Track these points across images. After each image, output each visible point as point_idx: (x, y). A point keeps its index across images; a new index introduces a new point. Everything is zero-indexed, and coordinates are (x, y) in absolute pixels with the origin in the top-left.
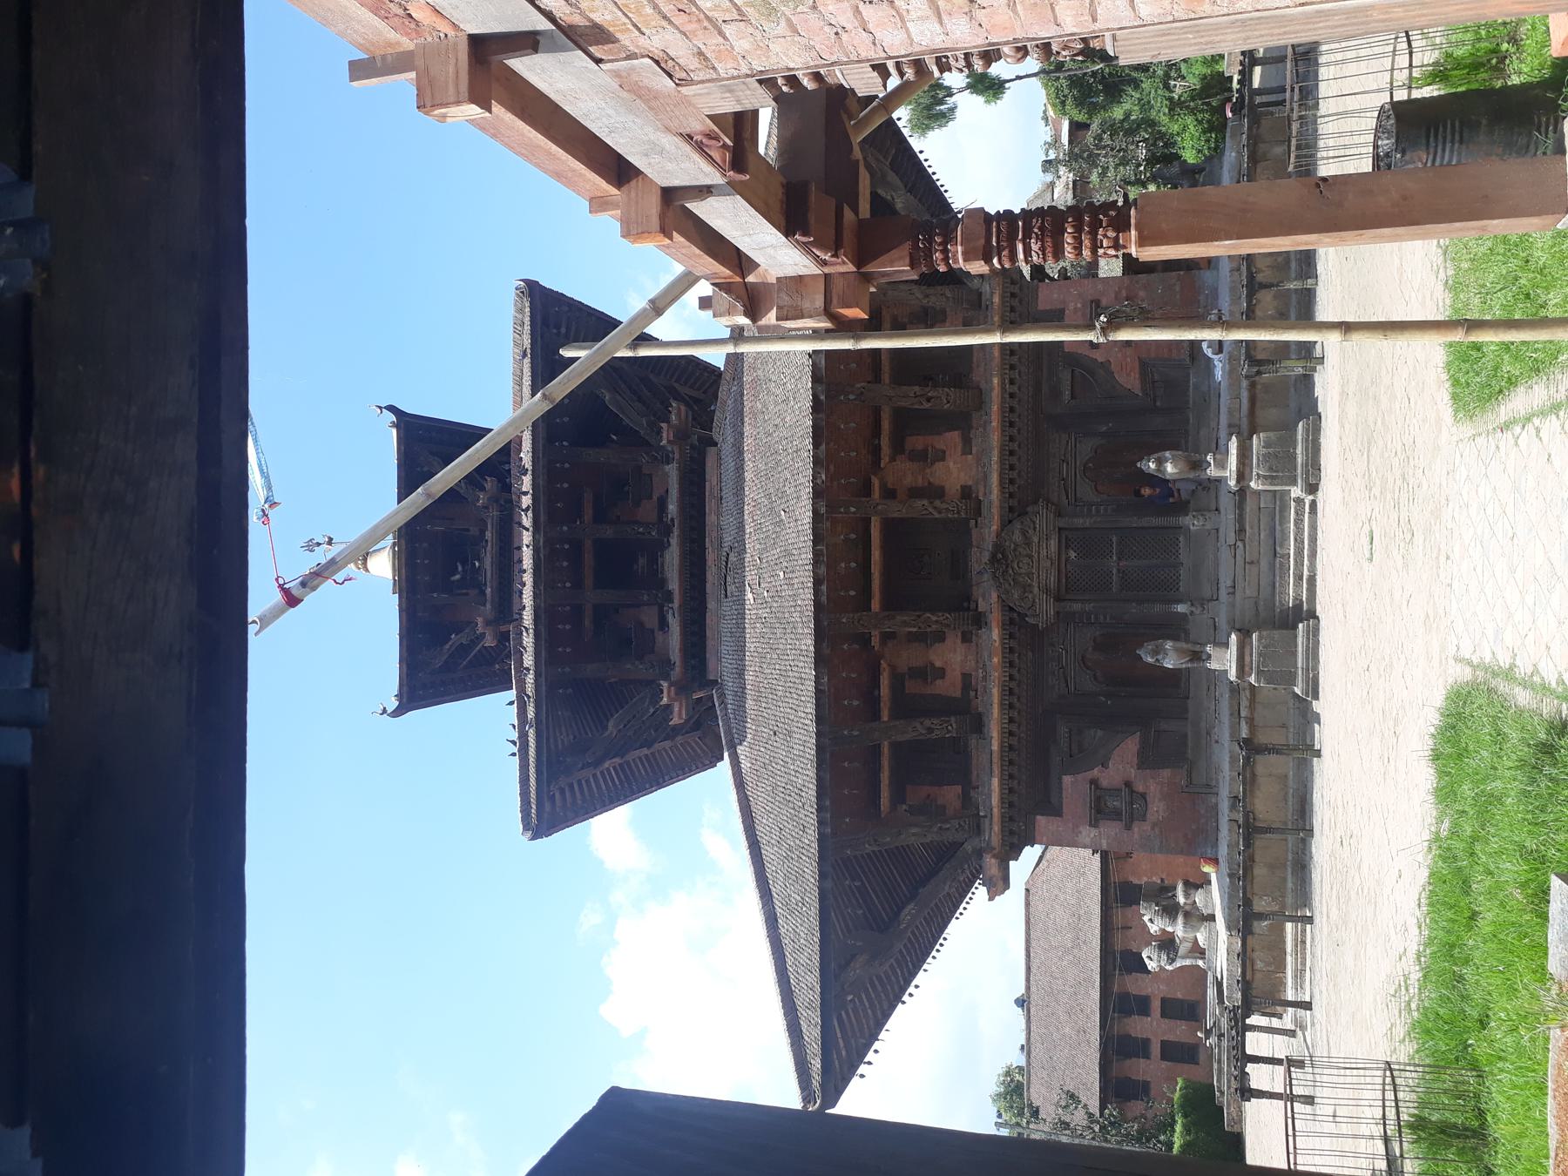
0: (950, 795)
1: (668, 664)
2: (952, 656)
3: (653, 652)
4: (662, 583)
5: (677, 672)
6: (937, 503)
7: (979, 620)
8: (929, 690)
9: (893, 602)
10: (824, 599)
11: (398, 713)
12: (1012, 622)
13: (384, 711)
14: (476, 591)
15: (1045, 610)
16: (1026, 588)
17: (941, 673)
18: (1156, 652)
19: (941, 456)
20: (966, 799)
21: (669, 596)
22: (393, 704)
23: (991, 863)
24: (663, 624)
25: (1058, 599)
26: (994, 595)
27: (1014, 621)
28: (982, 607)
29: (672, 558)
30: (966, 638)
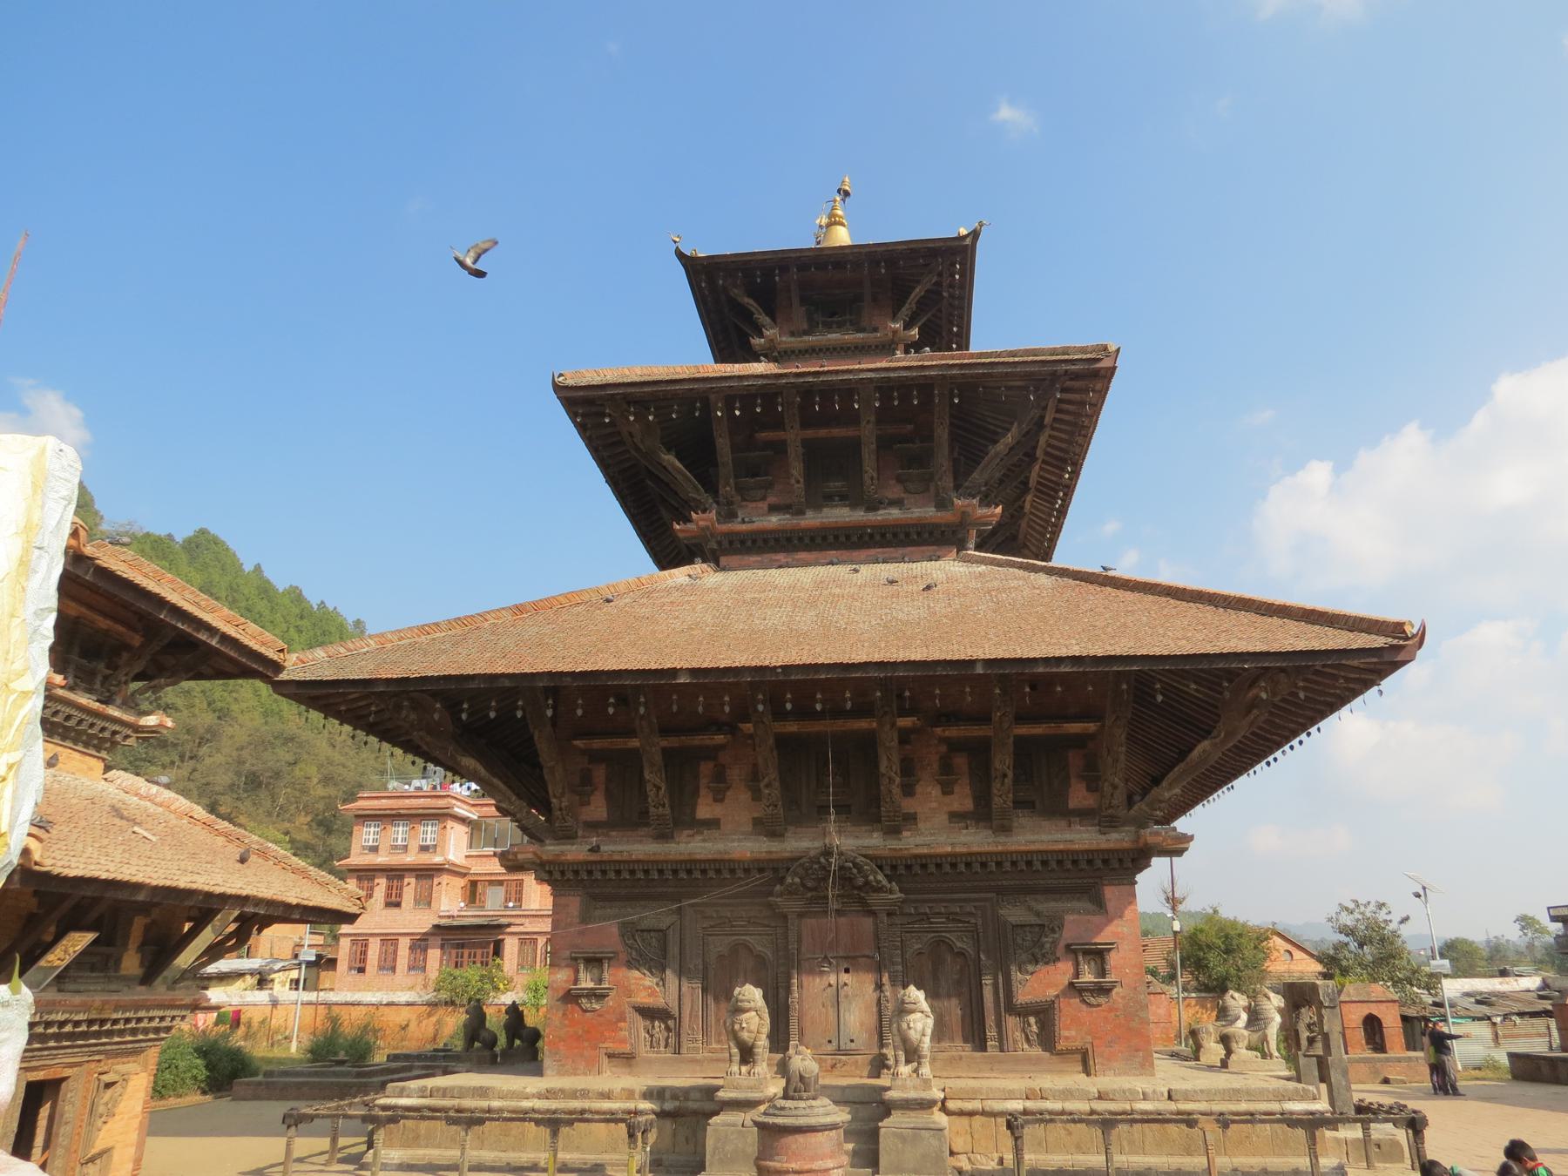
0: (598, 808)
1: (731, 516)
3: (744, 499)
4: (818, 507)
5: (725, 527)
7: (774, 834)
8: (703, 782)
12: (775, 870)
14: (805, 326)
19: (947, 790)
20: (593, 826)
21: (801, 512)
23: (529, 851)
24: (773, 509)
27: (774, 869)
29: (840, 515)
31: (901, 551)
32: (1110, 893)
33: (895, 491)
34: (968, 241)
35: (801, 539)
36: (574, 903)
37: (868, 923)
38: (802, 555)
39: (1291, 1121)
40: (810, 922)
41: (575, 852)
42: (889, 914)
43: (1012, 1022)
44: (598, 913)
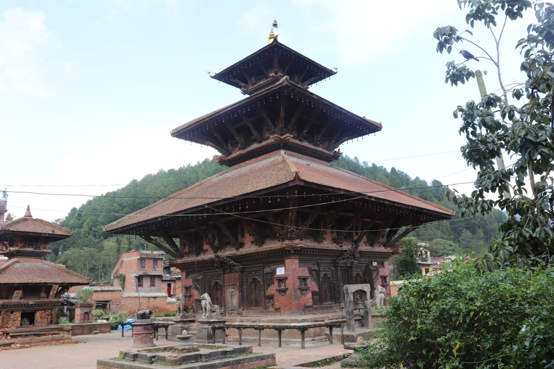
4: (249, 146)
22: (213, 75)
24: (240, 149)
29: (255, 146)
31: (269, 154)
32: (287, 261)
33: (267, 134)
34: (275, 43)
35: (244, 157)
36: (184, 274)
37: (237, 274)
38: (247, 162)
39: (275, 328)
40: (226, 276)
41: (179, 261)
42: (242, 272)
43: (267, 301)
44: (190, 276)
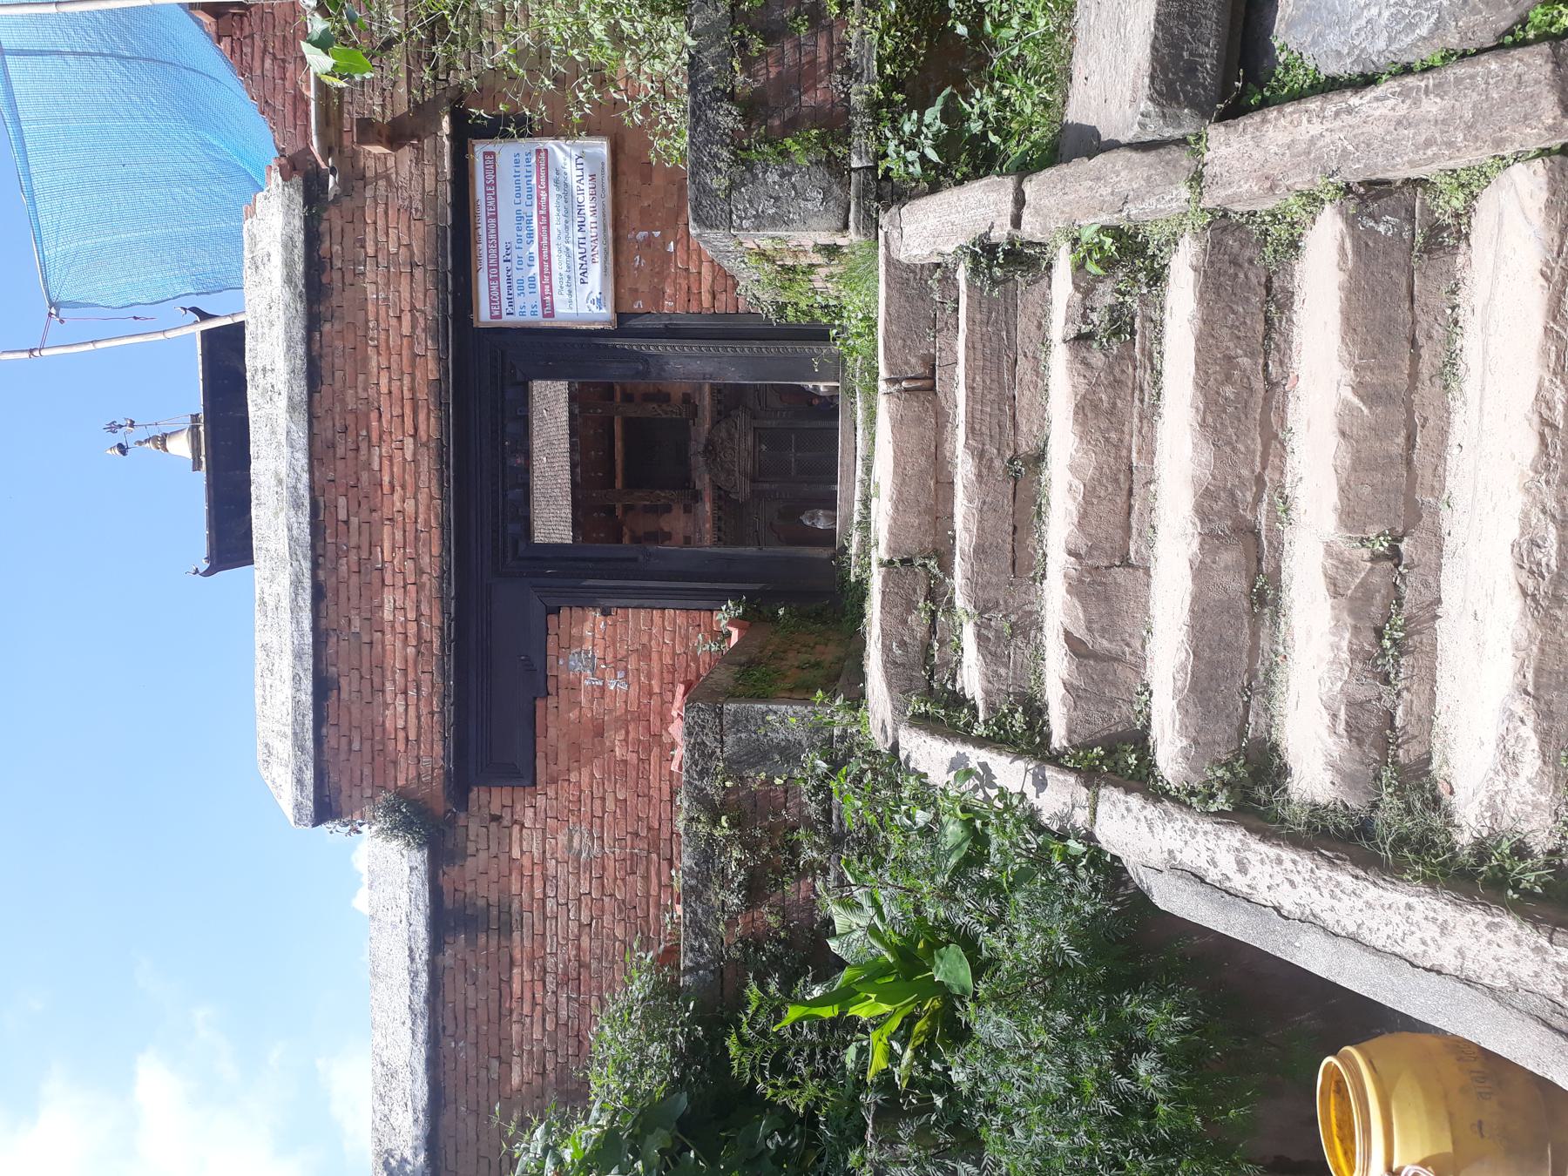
2: (676, 523)
6: (664, 406)
7: (697, 497)
9: (632, 483)
10: (579, 479)
11: (208, 573)
12: (720, 497)
13: (197, 571)
15: (743, 489)
16: (730, 472)
17: (668, 536)
18: (812, 518)
25: (753, 481)
26: (707, 477)
27: (722, 498)
28: (698, 486)
30: (687, 510)
